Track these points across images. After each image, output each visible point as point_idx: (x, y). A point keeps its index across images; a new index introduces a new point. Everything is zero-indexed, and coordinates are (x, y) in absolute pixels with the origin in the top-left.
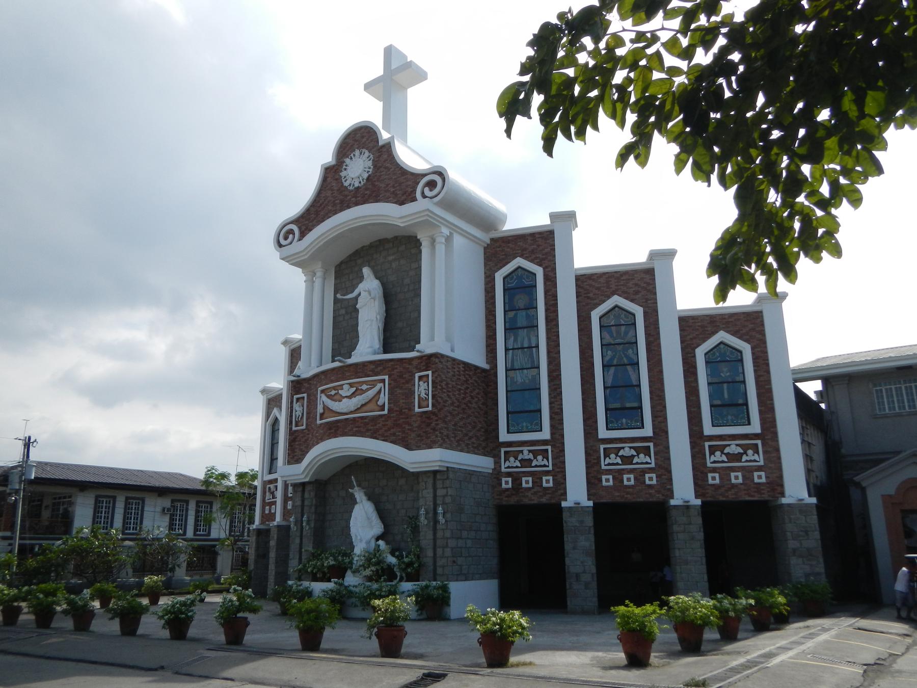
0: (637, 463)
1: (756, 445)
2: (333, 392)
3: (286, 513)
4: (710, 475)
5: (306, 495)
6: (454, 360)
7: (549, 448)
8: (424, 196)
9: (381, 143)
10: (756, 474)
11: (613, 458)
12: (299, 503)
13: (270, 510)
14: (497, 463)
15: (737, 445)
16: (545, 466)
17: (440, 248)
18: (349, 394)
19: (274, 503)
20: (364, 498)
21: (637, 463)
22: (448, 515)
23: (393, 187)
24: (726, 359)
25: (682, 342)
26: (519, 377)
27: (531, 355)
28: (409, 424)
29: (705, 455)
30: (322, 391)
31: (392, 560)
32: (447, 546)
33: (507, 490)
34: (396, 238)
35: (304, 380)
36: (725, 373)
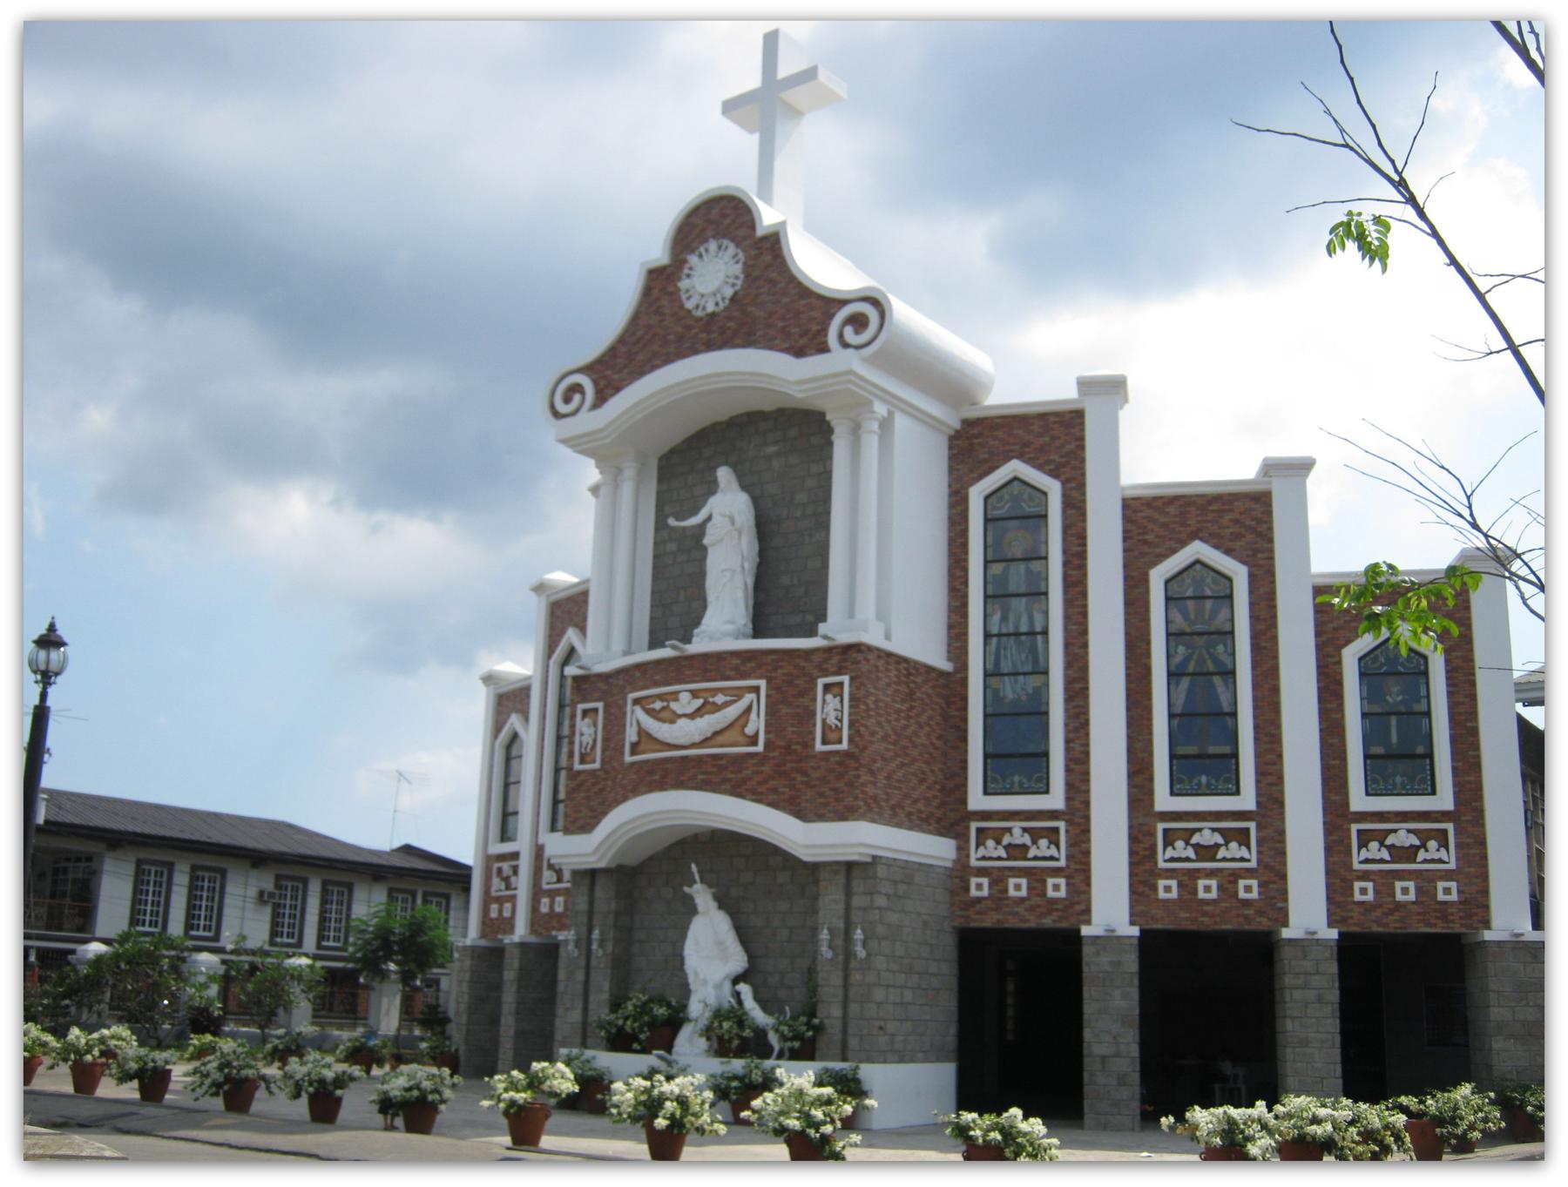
0: (1224, 859)
1: (1445, 832)
2: (658, 705)
3: (537, 921)
4: (1357, 885)
5: (598, 893)
6: (889, 655)
7: (1062, 825)
8: (845, 345)
9: (760, 233)
10: (1441, 885)
11: (1180, 849)
12: (582, 905)
13: (500, 912)
14: (963, 850)
15: (1409, 831)
16: (1052, 858)
17: (871, 444)
18: (690, 710)
19: (512, 899)
20: (713, 904)
21: (1224, 859)
22: (873, 944)
23: (783, 318)
24: (1393, 675)
25: (1318, 634)
26: (1009, 689)
27: (1033, 650)
28: (804, 773)
29: (1349, 847)
30: (636, 701)
33: (979, 900)
34: (781, 412)
35: (600, 676)
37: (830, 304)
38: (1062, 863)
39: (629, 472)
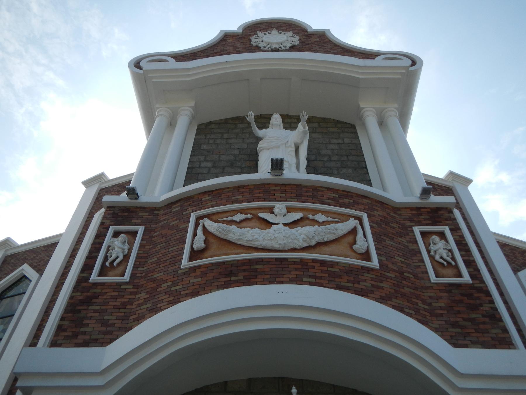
2: (238, 217)
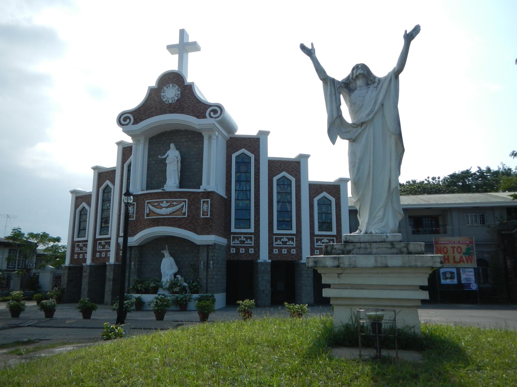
1: (334, 240)
2: (156, 204)
5: (133, 252)
6: (218, 194)
7: (253, 236)
8: (211, 117)
9: (186, 84)
11: (279, 242)
14: (229, 241)
16: (250, 244)
22: (215, 265)
26: (241, 203)
27: (247, 194)
30: (148, 203)
31: (186, 284)
32: (213, 278)
33: (233, 253)
34: (186, 130)
36: (324, 210)
37: (206, 106)
38: (253, 245)
39: (142, 142)
